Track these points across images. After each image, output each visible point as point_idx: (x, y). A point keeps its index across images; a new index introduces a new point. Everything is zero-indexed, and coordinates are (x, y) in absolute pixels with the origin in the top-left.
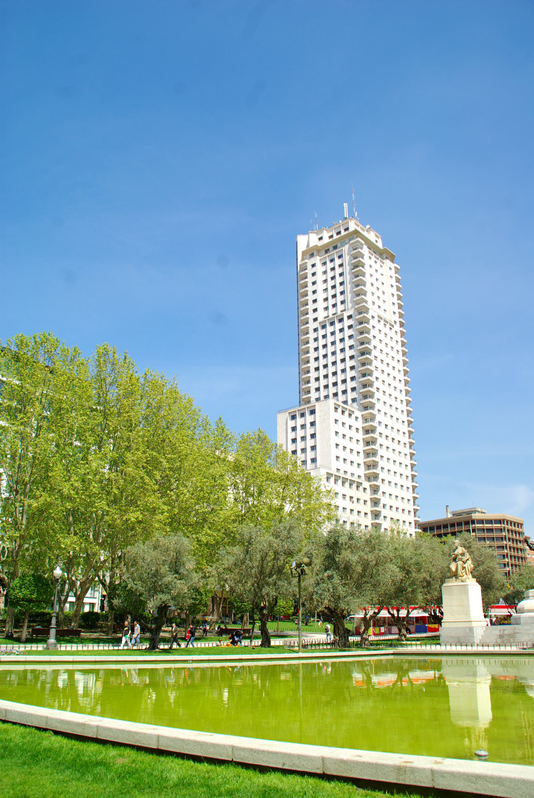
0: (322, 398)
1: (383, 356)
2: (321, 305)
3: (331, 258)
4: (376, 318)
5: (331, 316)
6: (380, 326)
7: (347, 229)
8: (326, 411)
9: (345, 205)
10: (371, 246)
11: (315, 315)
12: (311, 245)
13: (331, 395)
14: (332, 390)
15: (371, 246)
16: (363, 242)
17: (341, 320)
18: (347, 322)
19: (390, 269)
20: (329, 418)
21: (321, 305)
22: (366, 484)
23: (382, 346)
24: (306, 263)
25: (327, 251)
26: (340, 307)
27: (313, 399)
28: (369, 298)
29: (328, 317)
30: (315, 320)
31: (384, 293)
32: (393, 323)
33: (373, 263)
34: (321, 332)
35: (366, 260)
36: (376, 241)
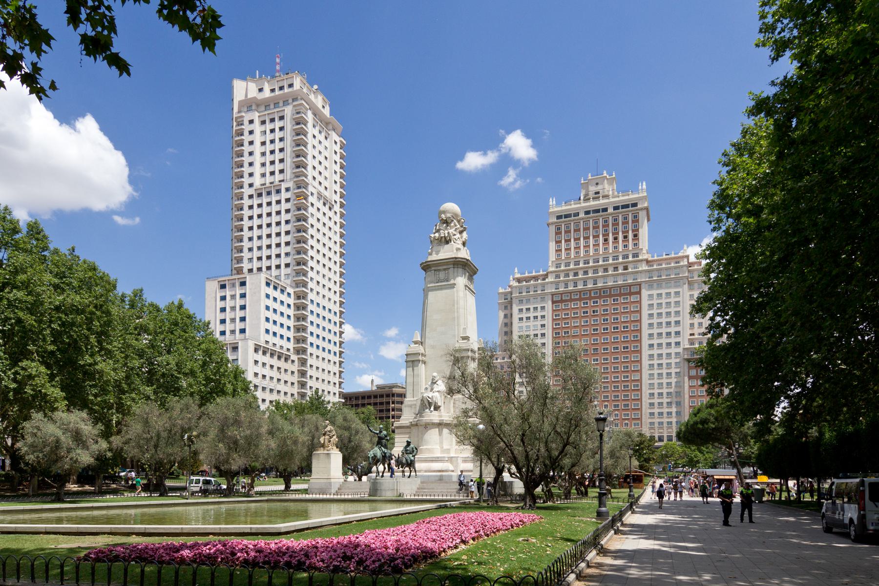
0: (255, 270)
1: (319, 236)
2: (257, 170)
3: (272, 117)
5: (268, 185)
7: (291, 86)
8: (256, 284)
11: (251, 180)
12: (249, 96)
13: (264, 269)
14: (265, 263)
17: (278, 191)
18: (284, 195)
20: (260, 292)
21: (257, 170)
22: (294, 357)
23: (319, 226)
24: (242, 117)
25: (267, 107)
27: (245, 270)
28: (310, 172)
31: (326, 168)
35: (311, 130)
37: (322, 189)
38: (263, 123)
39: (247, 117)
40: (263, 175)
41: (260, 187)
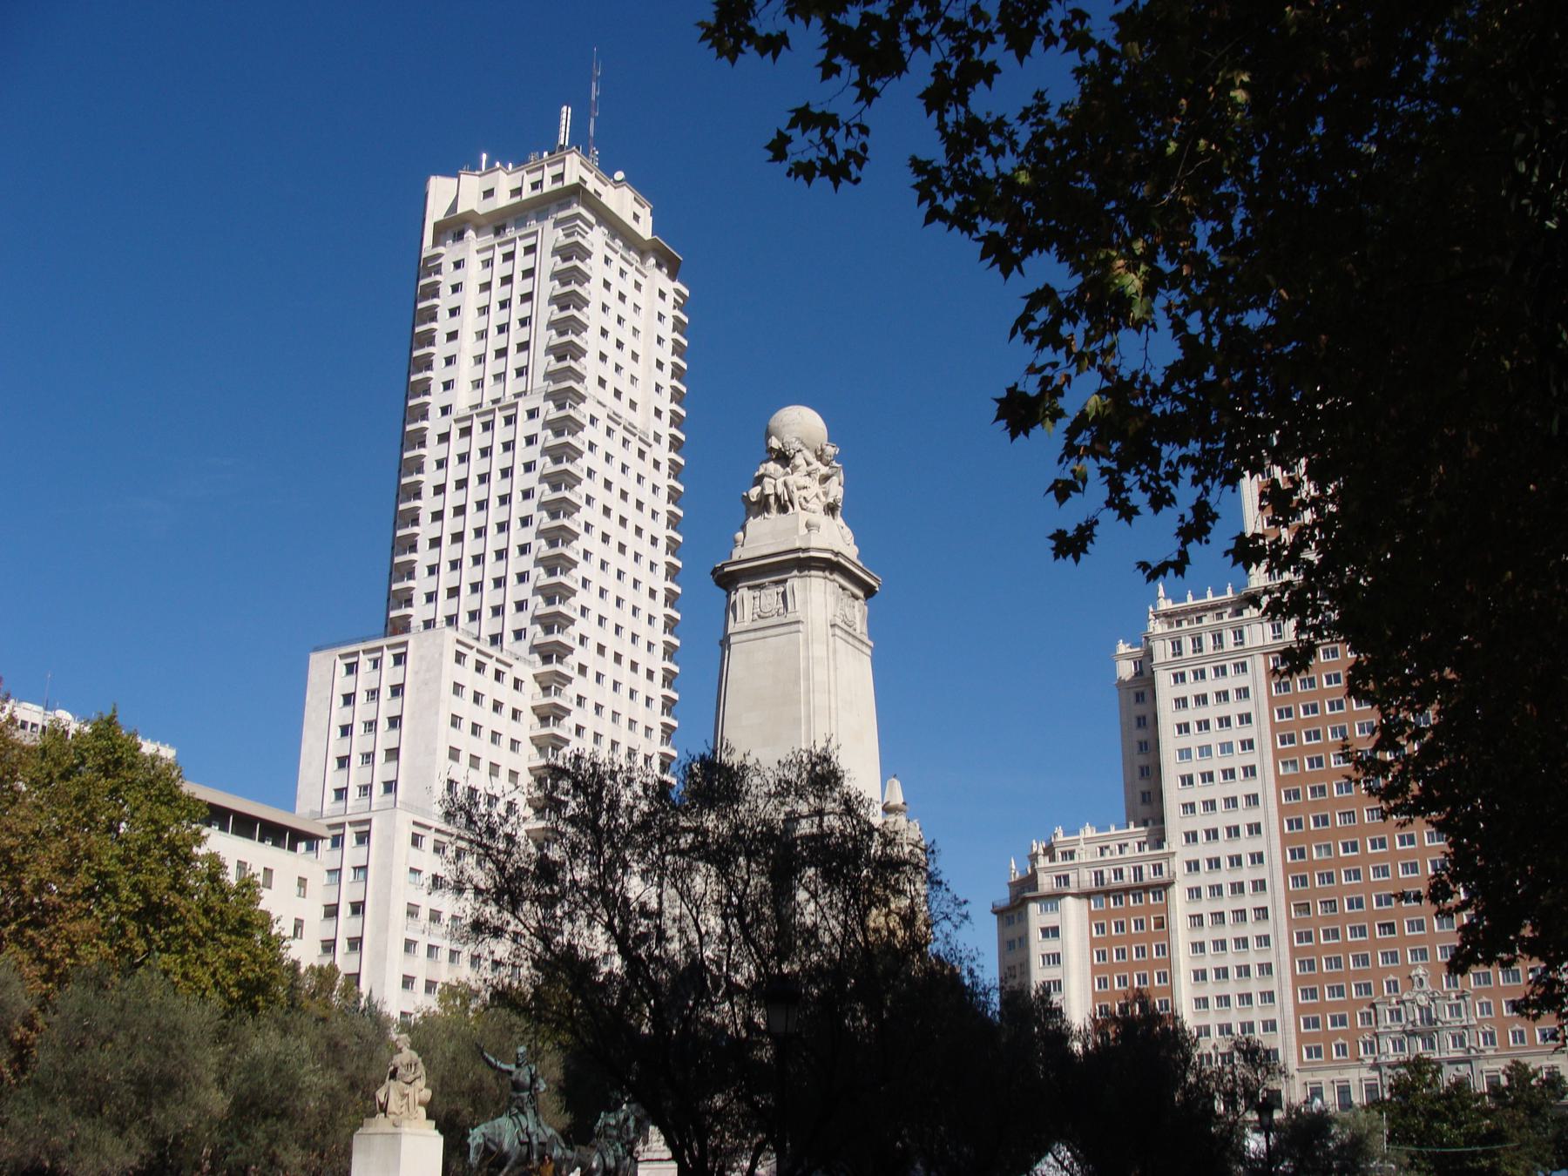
2: (465, 371)
4: (603, 423)
5: (487, 406)
6: (614, 445)
9: (566, 112)
10: (617, 228)
15: (617, 228)
16: (592, 219)
19: (662, 295)
26: (513, 384)
29: (480, 405)
30: (445, 411)
32: (651, 441)
33: (612, 275)
34: (457, 445)
36: (636, 217)
37: (622, 407)
38: (488, 263)
39: (449, 252)
40: (478, 384)
41: (468, 412)
